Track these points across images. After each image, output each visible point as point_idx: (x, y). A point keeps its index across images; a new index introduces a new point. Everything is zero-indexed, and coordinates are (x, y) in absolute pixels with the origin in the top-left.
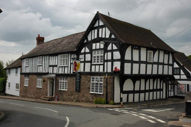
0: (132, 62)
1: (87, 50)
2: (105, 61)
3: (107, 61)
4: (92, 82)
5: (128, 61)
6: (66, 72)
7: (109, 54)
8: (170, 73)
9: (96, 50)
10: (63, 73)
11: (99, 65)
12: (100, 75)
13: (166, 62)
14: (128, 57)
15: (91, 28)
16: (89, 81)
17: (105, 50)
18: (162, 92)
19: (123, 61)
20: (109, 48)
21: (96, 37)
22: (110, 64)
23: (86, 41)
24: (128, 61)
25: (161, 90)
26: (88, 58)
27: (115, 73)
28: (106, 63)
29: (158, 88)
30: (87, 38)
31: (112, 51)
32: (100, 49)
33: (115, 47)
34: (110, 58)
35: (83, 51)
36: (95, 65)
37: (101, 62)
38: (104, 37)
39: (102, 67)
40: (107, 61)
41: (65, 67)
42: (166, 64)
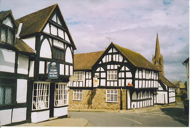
0: (139, 79)
1: (102, 70)
2: (118, 78)
3: (121, 78)
4: (107, 93)
5: (137, 79)
6: (81, 86)
7: (123, 73)
8: (157, 87)
9: (110, 70)
10: (84, 86)
11: (114, 81)
12: (115, 89)
13: (155, 79)
14: (136, 77)
15: (106, 53)
16: (105, 93)
17: (119, 70)
18: (151, 100)
19: (133, 79)
20: (123, 69)
21: (110, 60)
22: (123, 80)
23: (100, 63)
24: (137, 79)
25: (151, 99)
26: (103, 75)
27: (126, 87)
28: (120, 80)
29: (149, 97)
30: (101, 61)
31: (125, 72)
32: (114, 70)
33: (127, 69)
34: (123, 76)
35: (98, 70)
36: (110, 81)
37: (115, 79)
38: (117, 61)
39: (116, 83)
40: (121, 78)
41: (79, 82)
42: (155, 80)
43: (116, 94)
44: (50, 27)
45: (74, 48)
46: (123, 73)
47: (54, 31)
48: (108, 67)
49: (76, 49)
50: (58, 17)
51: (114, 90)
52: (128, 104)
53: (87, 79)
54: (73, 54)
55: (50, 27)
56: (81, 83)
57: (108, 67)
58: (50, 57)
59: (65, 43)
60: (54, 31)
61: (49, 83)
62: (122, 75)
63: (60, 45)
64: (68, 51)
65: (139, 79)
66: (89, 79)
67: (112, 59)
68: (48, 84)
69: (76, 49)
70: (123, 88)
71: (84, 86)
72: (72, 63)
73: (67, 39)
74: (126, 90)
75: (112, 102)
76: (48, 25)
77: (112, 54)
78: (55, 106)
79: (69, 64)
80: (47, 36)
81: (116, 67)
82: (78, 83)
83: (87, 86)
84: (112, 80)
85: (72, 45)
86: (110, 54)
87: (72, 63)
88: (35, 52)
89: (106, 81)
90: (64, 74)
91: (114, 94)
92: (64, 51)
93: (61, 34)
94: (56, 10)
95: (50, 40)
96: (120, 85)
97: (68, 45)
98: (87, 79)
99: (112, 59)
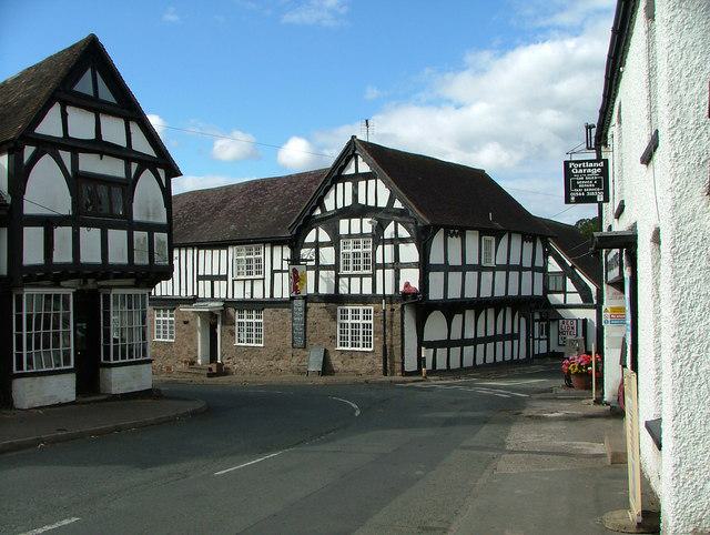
0: (446, 268)
1: (324, 237)
2: (376, 267)
3: (384, 266)
4: (339, 321)
5: (437, 268)
6: (258, 295)
7: (389, 248)
8: (539, 292)
9: (350, 236)
11: (361, 276)
12: (365, 303)
13: (527, 263)
14: (436, 257)
15: (335, 175)
16: (335, 318)
17: (377, 238)
18: (516, 342)
19: (425, 267)
20: (389, 232)
21: (349, 202)
22: (390, 273)
23: (318, 212)
24: (437, 268)
25: (513, 337)
26: (328, 255)
27: (405, 298)
28: (379, 272)
29: (508, 331)
30: (321, 204)
31: (396, 241)
32: (362, 235)
33: (403, 233)
34: (389, 259)
35: (311, 237)
36: (350, 276)
37: (366, 268)
38: (371, 203)
39: (368, 282)
40: (384, 266)
41: (252, 280)
42: (527, 269)
43: (369, 322)
44: (64, 116)
45: (173, 171)
46: (389, 248)
47: (82, 125)
48: (344, 226)
49: (177, 173)
50: (103, 77)
51: (361, 308)
52: (477, 355)
53: (278, 271)
54: (166, 191)
55: (64, 116)
56: (258, 286)
57: (344, 226)
58: (64, 206)
59: (125, 154)
60: (82, 125)
61: (70, 292)
62: (385, 254)
63: (114, 168)
64: (147, 186)
65: (446, 268)
66: (281, 271)
67: (355, 196)
68: (66, 297)
69: (177, 173)
70: (390, 299)
71: (268, 296)
72: (163, 220)
73: (141, 145)
74: (399, 306)
75: (357, 349)
76: (56, 110)
77: (356, 178)
78: (15, 371)
79: (151, 228)
80: (48, 146)
81: (368, 225)
82: (248, 284)
83: (277, 295)
84: (355, 272)
85: (164, 165)
86: (349, 178)
87: (163, 220)
88: (9, 200)
89: (337, 277)
90: (100, 261)
91: (361, 321)
92: (128, 186)
93: (114, 130)
94: (91, 55)
95: (66, 156)
96: (379, 291)
97: (145, 163)
98: (278, 271)
99: (355, 196)
